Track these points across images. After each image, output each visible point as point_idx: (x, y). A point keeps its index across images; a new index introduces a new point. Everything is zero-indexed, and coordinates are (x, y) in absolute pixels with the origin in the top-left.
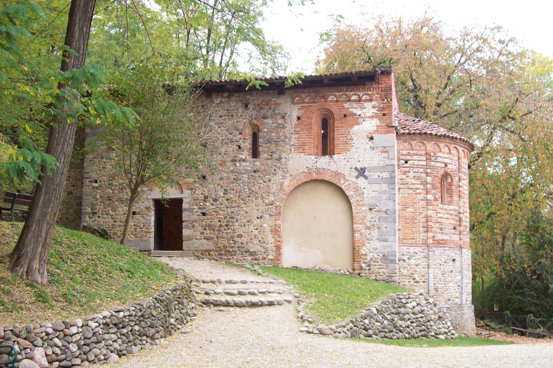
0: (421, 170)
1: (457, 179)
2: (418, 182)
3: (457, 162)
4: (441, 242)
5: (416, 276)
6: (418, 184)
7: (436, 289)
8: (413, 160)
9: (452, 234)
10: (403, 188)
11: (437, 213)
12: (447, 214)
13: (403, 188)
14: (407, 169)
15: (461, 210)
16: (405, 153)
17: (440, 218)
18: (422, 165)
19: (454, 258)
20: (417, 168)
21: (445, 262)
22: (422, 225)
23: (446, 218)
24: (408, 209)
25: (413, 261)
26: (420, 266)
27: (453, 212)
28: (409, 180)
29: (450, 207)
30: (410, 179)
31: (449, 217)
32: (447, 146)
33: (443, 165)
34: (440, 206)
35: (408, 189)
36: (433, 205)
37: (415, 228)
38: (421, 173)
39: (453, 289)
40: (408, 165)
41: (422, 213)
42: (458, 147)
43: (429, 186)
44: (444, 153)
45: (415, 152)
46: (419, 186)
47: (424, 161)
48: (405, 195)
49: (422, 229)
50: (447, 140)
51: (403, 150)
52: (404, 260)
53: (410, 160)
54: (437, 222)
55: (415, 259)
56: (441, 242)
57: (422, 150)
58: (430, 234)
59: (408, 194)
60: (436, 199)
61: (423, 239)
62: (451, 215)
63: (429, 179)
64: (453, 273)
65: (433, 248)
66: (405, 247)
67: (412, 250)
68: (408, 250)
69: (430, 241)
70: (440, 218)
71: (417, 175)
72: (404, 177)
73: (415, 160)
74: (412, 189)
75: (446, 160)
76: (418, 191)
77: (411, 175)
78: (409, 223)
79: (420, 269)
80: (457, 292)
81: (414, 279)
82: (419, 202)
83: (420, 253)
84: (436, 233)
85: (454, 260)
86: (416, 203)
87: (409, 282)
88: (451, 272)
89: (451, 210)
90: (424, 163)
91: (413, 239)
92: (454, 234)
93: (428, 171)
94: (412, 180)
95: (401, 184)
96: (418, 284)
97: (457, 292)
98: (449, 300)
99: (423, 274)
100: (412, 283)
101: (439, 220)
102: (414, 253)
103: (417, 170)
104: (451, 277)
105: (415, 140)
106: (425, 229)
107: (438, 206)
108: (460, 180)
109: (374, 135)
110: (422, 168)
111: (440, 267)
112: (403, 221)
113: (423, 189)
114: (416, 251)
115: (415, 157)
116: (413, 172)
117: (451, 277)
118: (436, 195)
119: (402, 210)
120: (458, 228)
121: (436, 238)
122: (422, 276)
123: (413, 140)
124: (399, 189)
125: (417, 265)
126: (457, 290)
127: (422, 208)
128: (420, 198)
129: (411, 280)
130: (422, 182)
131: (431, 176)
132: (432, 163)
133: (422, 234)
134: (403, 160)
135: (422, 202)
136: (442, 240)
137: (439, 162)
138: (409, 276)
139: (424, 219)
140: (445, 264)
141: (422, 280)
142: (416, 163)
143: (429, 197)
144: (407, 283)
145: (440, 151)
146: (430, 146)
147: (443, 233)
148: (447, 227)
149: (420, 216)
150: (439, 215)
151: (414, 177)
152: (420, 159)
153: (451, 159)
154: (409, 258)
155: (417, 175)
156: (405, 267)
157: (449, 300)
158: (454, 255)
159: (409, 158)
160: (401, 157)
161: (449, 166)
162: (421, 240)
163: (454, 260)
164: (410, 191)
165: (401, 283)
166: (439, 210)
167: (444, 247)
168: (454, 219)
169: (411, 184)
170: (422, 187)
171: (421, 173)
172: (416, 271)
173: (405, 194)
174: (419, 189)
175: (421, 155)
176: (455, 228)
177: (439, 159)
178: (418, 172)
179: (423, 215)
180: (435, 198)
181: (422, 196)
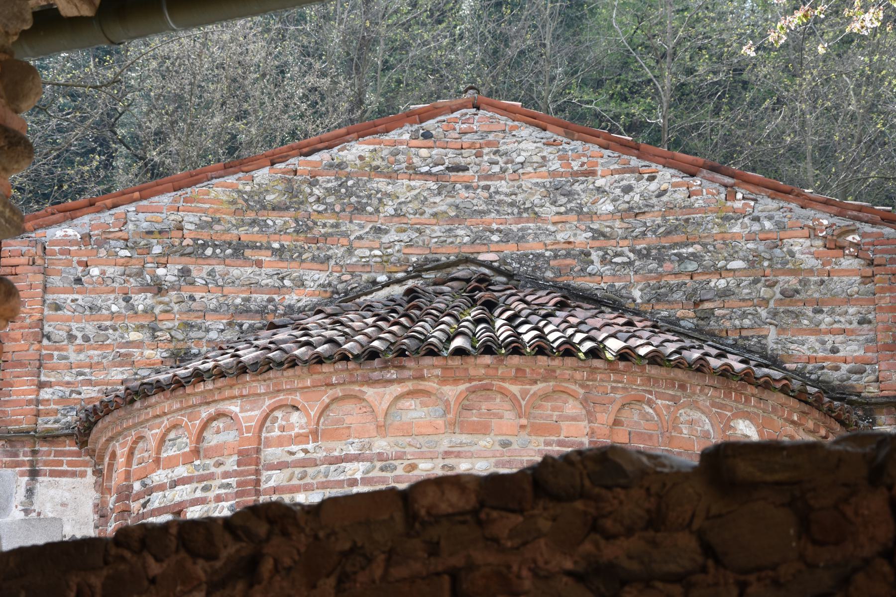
50: (161, 403)
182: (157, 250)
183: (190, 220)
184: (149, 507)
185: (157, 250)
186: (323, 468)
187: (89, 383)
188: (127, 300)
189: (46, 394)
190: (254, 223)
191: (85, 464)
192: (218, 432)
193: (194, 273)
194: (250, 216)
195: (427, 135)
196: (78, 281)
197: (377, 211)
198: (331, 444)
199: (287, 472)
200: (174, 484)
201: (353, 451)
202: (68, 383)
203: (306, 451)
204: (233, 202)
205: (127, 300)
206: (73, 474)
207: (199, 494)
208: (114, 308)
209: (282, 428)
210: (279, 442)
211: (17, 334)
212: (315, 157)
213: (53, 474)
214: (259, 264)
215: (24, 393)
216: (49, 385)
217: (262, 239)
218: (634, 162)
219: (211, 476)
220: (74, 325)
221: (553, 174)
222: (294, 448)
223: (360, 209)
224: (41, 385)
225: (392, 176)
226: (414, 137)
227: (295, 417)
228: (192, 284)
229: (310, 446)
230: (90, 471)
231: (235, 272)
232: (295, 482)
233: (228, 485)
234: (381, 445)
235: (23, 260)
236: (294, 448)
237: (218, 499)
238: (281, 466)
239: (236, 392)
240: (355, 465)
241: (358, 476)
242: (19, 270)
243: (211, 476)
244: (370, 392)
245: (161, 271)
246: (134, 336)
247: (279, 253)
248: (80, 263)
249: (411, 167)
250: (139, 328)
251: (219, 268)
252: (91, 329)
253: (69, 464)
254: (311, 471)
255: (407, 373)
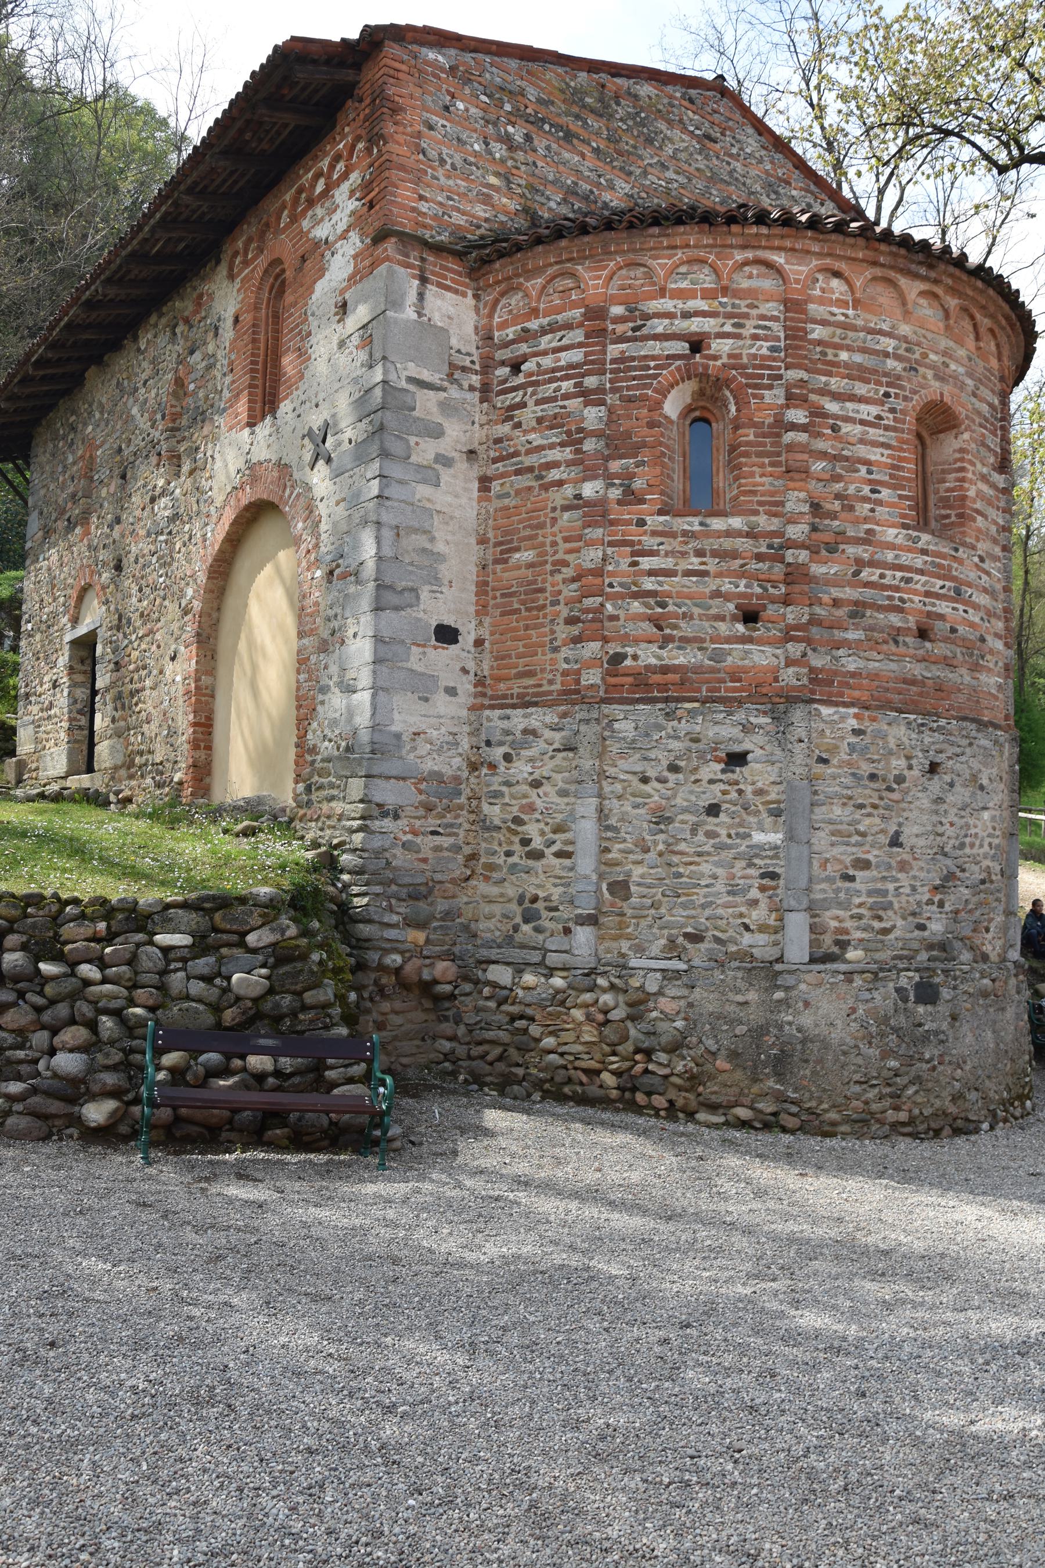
0: (567, 386)
1: (774, 396)
2: (555, 437)
3: (777, 328)
4: (657, 678)
5: (532, 830)
6: (552, 446)
7: (620, 888)
8: (536, 354)
9: (728, 640)
10: (503, 476)
11: (634, 554)
12: (700, 553)
13: (503, 476)
14: (517, 397)
15: (797, 531)
16: (511, 336)
17: (651, 573)
18: (571, 366)
19: (737, 748)
20: (551, 381)
21: (674, 768)
22: (565, 612)
23: (688, 573)
24: (517, 556)
25: (521, 769)
26: (546, 788)
27: (742, 544)
28: (520, 439)
29: (717, 524)
30: (525, 432)
31: (712, 565)
32: (703, 261)
33: (681, 347)
34: (654, 521)
35: (518, 472)
36: (612, 523)
37: (536, 627)
38: (566, 397)
39: (720, 887)
40: (521, 379)
41: (565, 564)
42: (779, 259)
43: (589, 445)
44: (682, 295)
45: (545, 321)
46: (555, 455)
47: (580, 345)
48: (506, 501)
49: (563, 632)
50: (691, 235)
51: (503, 325)
52: (492, 766)
53: (525, 359)
54: (635, 596)
55: (531, 760)
56: (657, 678)
57: (574, 305)
58: (592, 648)
59: (518, 492)
60: (630, 497)
61: (565, 673)
62: (721, 555)
63: (593, 416)
64: (723, 817)
65: (606, 709)
66: (498, 712)
67: (519, 720)
68: (505, 725)
69: (592, 677)
70: (651, 573)
71: (550, 409)
72: (505, 429)
73: (544, 353)
74: (530, 469)
75: (695, 325)
76: (555, 474)
77: (528, 416)
78: (517, 611)
79: (547, 797)
80: (754, 903)
81: (526, 842)
82: (554, 520)
83: (548, 734)
84: (626, 639)
85: (737, 759)
86: (541, 526)
87: (509, 854)
88: (713, 810)
89: (729, 533)
90: (576, 356)
91: (530, 674)
92: (750, 640)
93: (591, 382)
94: (532, 436)
95: (495, 461)
96: (538, 865)
97: (754, 903)
98: (695, 938)
99: (559, 817)
100: (515, 859)
101: (649, 584)
102: (525, 731)
103: (549, 390)
104: (711, 835)
105: (537, 271)
106: (575, 630)
107: (641, 523)
108: (792, 399)
109: (347, 296)
110: (567, 378)
111: (647, 788)
112: (496, 606)
113: (569, 463)
114: (534, 723)
115: (546, 342)
116: (538, 403)
117: (711, 835)
118: (631, 476)
119: (496, 562)
120: (771, 611)
121: (628, 662)
122: (554, 832)
123: (530, 274)
124: (484, 483)
125: (536, 784)
126: (754, 893)
127: (566, 540)
128: (559, 502)
129: (517, 847)
130: (569, 433)
131: (602, 403)
132: (614, 350)
133: (565, 652)
134: (503, 363)
135: (566, 515)
136: (665, 670)
137: (656, 337)
138: (509, 829)
139: (574, 586)
140: (672, 777)
141: (555, 848)
142: (547, 362)
143: (589, 490)
144: (500, 860)
145: (662, 292)
146: (598, 280)
147: (667, 640)
148: (697, 611)
149: (559, 578)
150: (646, 563)
151: (540, 420)
152: (565, 342)
153: (729, 316)
154: (507, 758)
155: (550, 409)
156: (497, 795)
157: (695, 938)
158: (736, 732)
159: (524, 348)
160: (501, 355)
161: (722, 347)
162: (559, 679)
163: (737, 759)
164: (525, 481)
165: (483, 860)
166: (650, 542)
167: (666, 700)
168: (742, 575)
169: (528, 452)
170: (568, 453)
171: (566, 397)
172: (531, 808)
173: (507, 495)
174: (555, 464)
175: (568, 326)
176: (750, 617)
177: (660, 326)
178: (553, 399)
179: (568, 572)
180: (628, 491)
181: (569, 491)
182: (508, 107)
183: (532, 93)
184: (645, 331)
185: (508, 107)
186: (862, 334)
187: (458, 210)
188: (487, 144)
189: (424, 207)
190: (577, 117)
191: (467, 286)
192: (750, 277)
193: (536, 142)
194: (575, 109)
195: (691, 101)
196: (447, 108)
197: (661, 148)
198: (869, 317)
199: (831, 329)
200: (687, 315)
201: (885, 327)
202: (440, 204)
203: (846, 316)
204: (562, 91)
205: (487, 144)
206: (456, 292)
207: (728, 328)
208: (476, 147)
209: (823, 290)
210: (821, 301)
211: (400, 138)
212: (619, 81)
213: (440, 285)
214: (583, 156)
215: (408, 198)
216: (426, 200)
217: (584, 134)
218: (812, 187)
219: (746, 316)
220: (445, 151)
221: (767, 172)
222: (835, 310)
223: (649, 141)
224: (421, 198)
225: (670, 123)
226: (683, 97)
227: (835, 283)
228: (535, 151)
229: (850, 312)
230: (470, 293)
231: (566, 155)
232: (837, 340)
233: (765, 328)
234: (905, 329)
235: (404, 68)
236: (835, 310)
237: (755, 337)
238: (824, 323)
239: (788, 243)
240: (887, 340)
241: (890, 350)
242: (401, 75)
243: (746, 316)
244: (903, 282)
245: (510, 129)
246: (493, 180)
247: (597, 151)
248: (448, 92)
249: (681, 121)
250: (497, 174)
251: (554, 146)
252: (458, 159)
253: (453, 280)
254: (850, 334)
255: (933, 275)
